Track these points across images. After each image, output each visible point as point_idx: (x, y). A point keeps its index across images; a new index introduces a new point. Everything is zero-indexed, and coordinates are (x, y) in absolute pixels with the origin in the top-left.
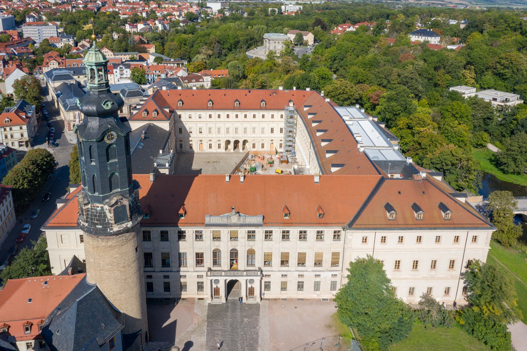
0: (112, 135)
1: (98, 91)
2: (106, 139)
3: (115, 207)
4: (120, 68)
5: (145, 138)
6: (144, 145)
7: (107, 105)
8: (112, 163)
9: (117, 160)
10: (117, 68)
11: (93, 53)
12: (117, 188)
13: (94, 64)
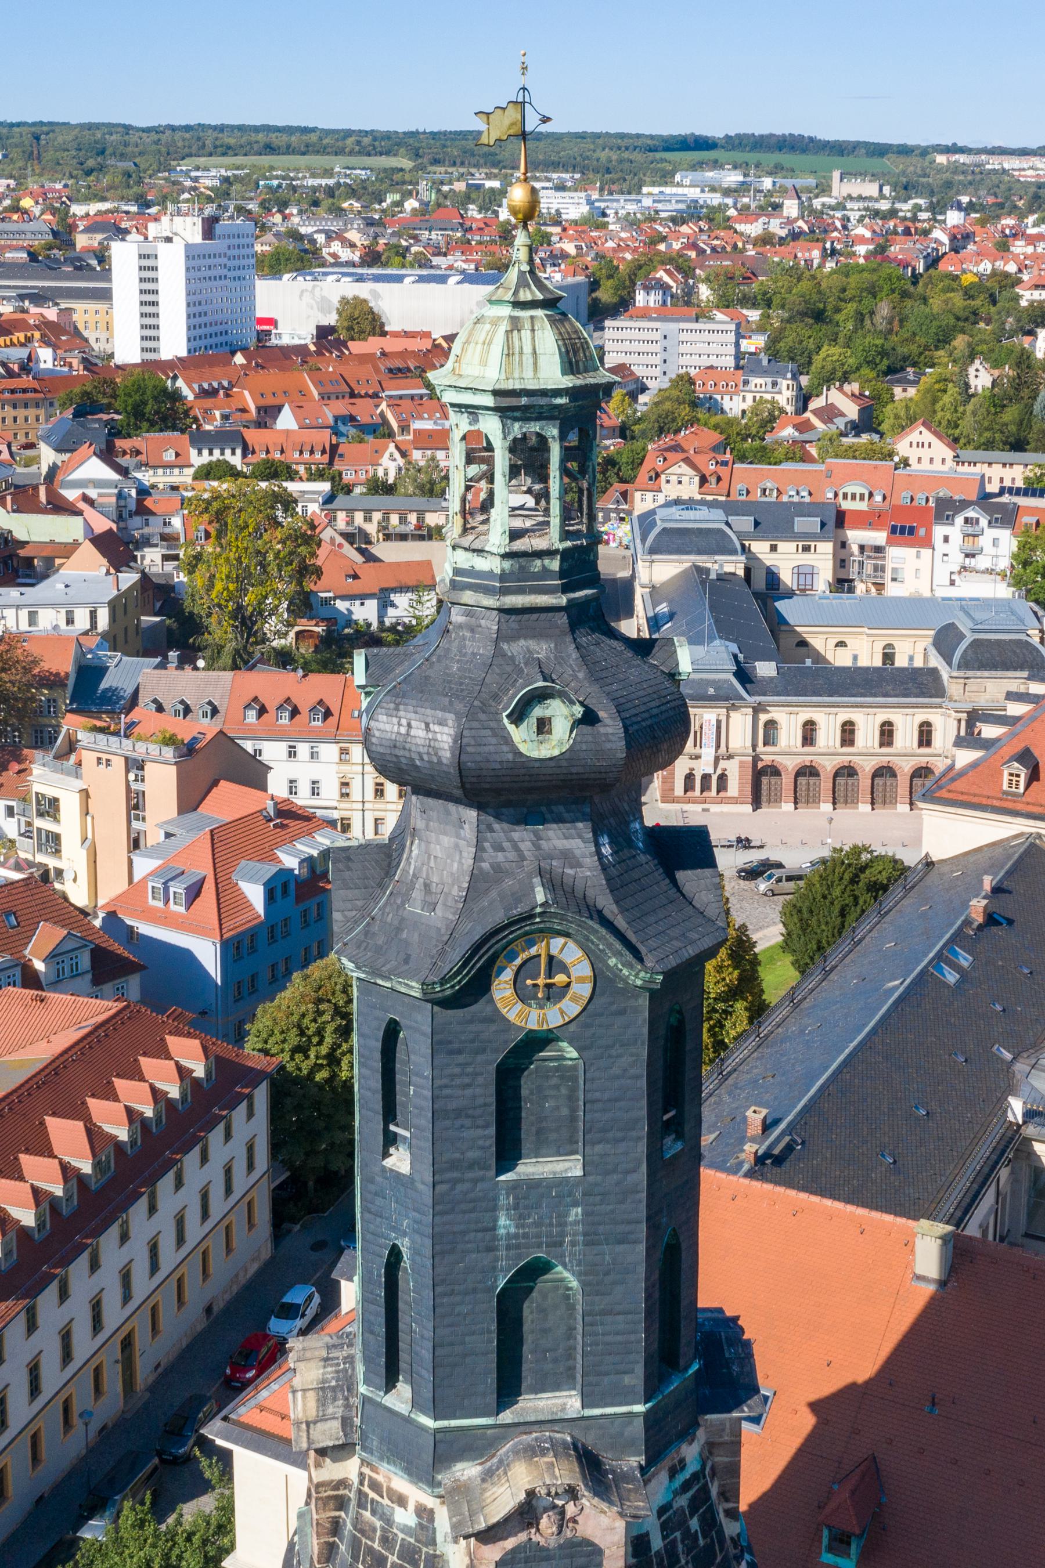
0: (554, 965)
1: (501, 610)
2: (502, 988)
3: (510, 1543)
4: (967, 520)
5: (991, 920)
6: (973, 966)
7: (543, 726)
8: (533, 1184)
9: (571, 1167)
10: (949, 520)
11: (495, 322)
12: (557, 1387)
13: (489, 401)
